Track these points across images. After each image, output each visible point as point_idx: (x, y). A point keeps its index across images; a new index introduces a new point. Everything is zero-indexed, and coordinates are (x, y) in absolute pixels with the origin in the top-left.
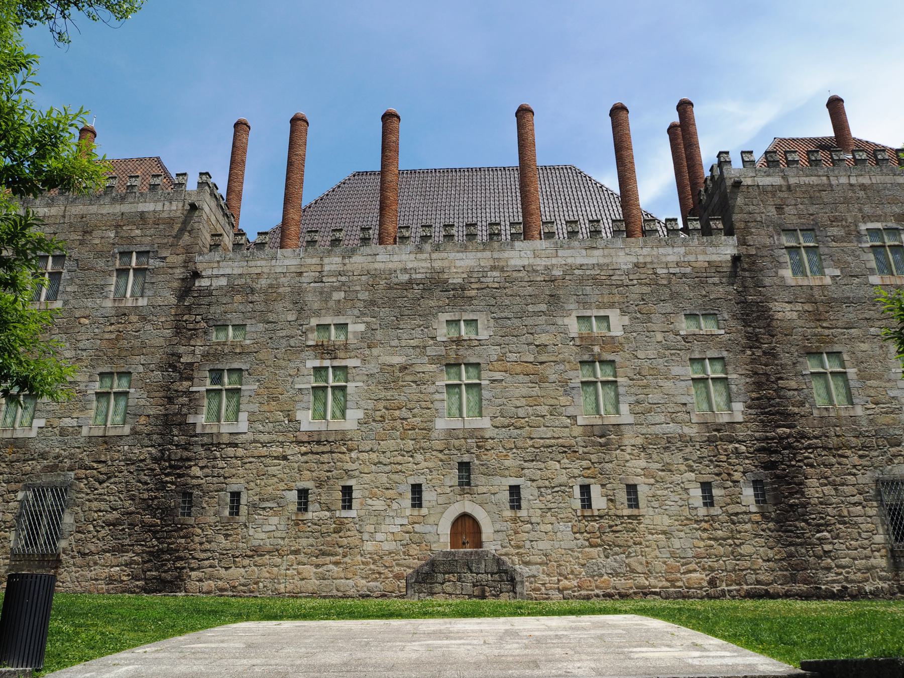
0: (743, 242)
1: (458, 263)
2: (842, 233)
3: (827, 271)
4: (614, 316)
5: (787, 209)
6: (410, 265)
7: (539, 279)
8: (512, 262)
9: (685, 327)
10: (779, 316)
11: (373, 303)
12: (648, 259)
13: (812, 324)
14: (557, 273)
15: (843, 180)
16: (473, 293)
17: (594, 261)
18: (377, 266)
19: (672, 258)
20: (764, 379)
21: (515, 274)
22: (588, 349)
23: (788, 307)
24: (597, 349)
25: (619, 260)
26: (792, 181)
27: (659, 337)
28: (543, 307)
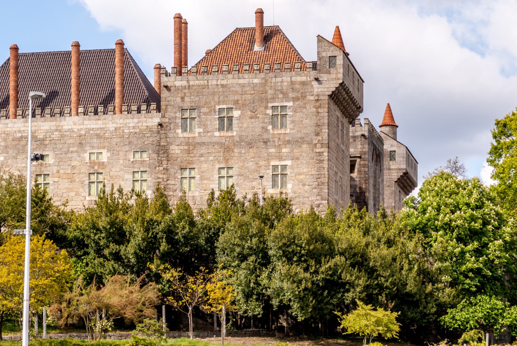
0: (163, 117)
1: (42, 128)
2: (207, 111)
3: (197, 130)
4: (104, 151)
5: (186, 98)
6: (22, 129)
7: (75, 135)
8: (64, 127)
9: (131, 157)
10: (173, 152)
11: (6, 147)
12: (122, 126)
13: (186, 155)
14: (83, 132)
15: (214, 82)
16: (48, 142)
17: (98, 126)
18: (8, 129)
19: (131, 125)
20: (161, 180)
21: (65, 133)
22: (93, 168)
23: (177, 148)
24: (96, 167)
25: (109, 126)
26: (191, 83)
27: (121, 162)
28: (75, 149)
